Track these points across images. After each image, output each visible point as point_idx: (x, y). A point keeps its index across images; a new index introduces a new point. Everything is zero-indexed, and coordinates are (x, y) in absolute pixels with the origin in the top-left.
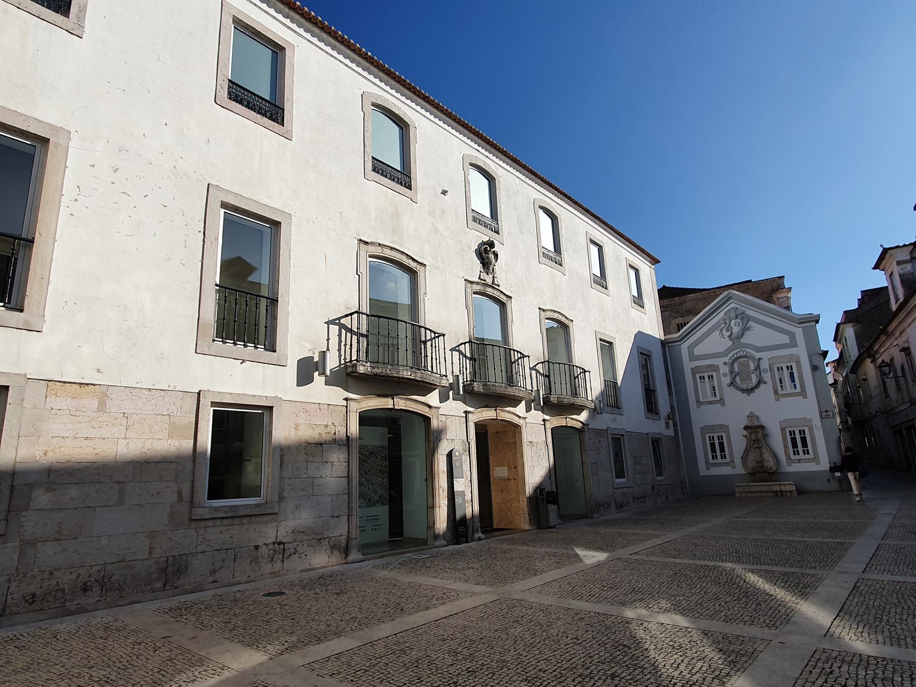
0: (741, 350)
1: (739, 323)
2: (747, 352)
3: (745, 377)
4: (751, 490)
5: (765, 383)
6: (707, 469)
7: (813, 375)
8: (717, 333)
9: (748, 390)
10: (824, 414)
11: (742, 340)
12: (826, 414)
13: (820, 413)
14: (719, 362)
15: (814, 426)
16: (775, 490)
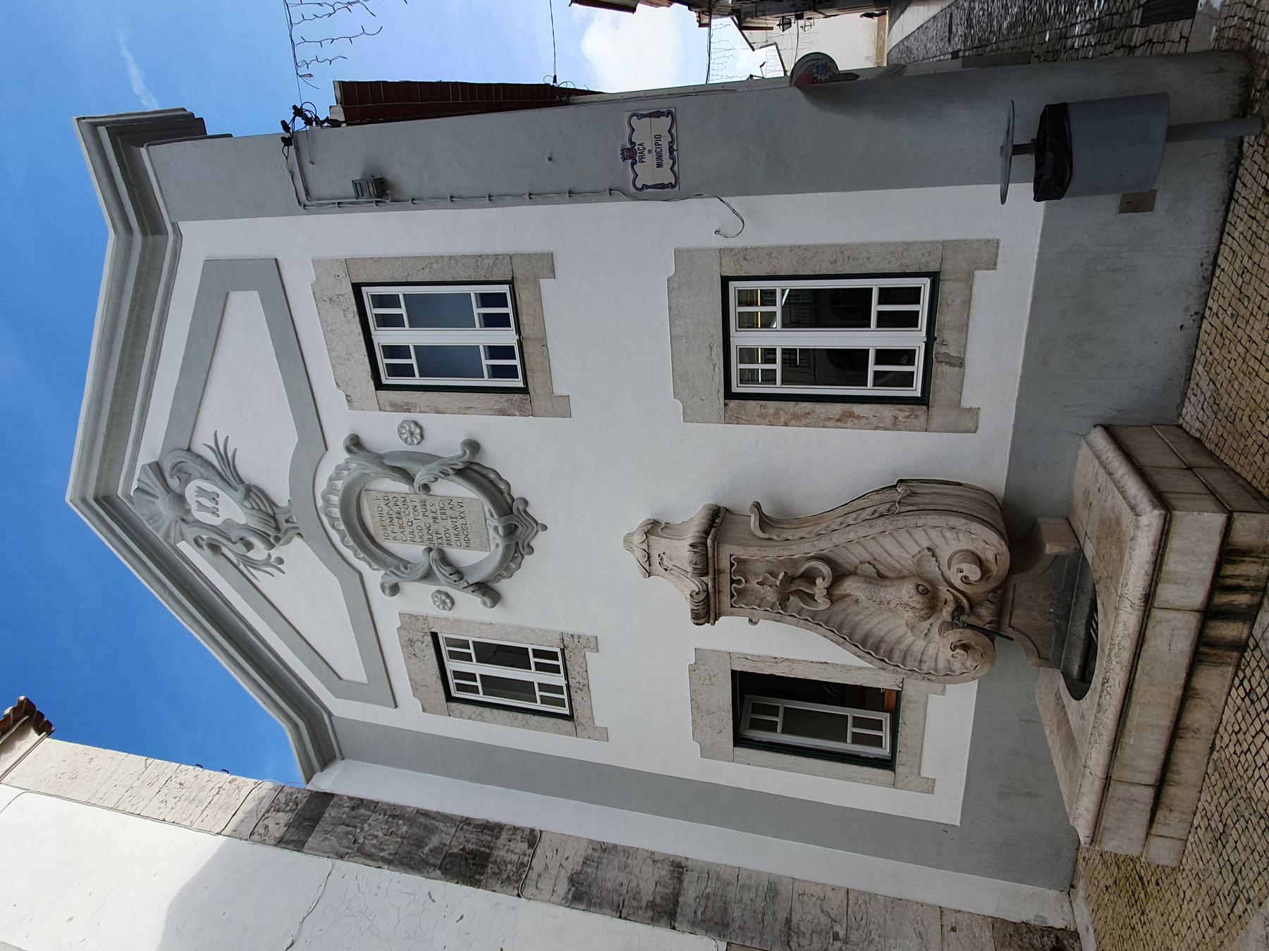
0: (328, 515)
1: (202, 491)
2: (331, 489)
3: (449, 524)
4: (1151, 779)
5: (473, 446)
6: (931, 791)
7: (415, 202)
8: (263, 580)
9: (510, 531)
10: (648, 172)
11: (282, 495)
12: (650, 159)
13: (642, 192)
14: (389, 611)
15: (721, 242)
16: (1183, 644)
